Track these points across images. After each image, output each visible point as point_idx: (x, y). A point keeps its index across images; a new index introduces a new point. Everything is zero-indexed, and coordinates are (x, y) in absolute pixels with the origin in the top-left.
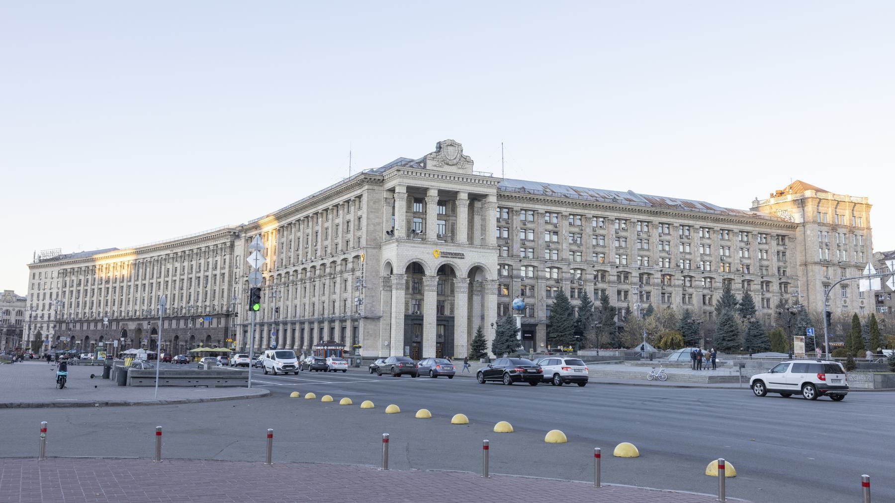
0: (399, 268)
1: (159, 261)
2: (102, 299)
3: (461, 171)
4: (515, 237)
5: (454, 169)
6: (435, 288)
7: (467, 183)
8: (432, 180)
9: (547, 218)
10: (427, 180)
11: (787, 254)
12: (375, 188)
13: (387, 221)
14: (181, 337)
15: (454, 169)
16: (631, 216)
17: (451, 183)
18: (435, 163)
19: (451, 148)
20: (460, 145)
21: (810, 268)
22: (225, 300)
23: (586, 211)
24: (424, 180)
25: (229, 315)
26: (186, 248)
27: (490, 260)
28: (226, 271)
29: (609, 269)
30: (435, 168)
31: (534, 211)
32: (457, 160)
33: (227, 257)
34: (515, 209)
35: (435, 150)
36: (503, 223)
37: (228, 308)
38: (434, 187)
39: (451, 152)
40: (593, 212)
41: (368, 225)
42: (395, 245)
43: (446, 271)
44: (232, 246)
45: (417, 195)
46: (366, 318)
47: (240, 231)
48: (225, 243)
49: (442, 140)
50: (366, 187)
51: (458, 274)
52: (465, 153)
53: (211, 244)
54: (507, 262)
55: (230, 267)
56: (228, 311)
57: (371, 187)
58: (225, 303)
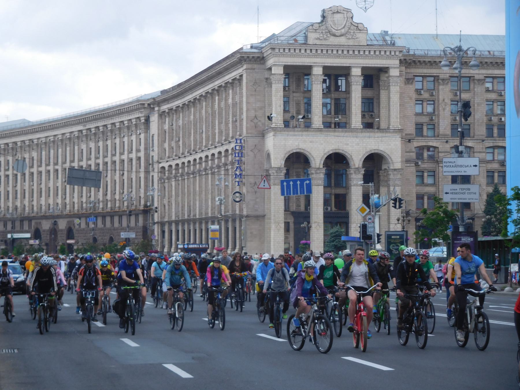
0: (278, 161)
1: (71, 140)
2: (10, 189)
3: (351, 42)
4: (441, 113)
5: (342, 40)
6: (321, 182)
7: (359, 56)
9: (489, 85)
10: (309, 56)
12: (255, 66)
14: (99, 239)
15: (342, 40)
17: (339, 57)
18: (317, 35)
19: (337, 16)
20: (348, 11)
22: (142, 191)
24: (305, 56)
25: (147, 211)
26: (100, 124)
27: (391, 147)
28: (142, 154)
30: (318, 42)
31: (470, 77)
32: (346, 29)
33: (142, 136)
34: (442, 76)
35: (319, 19)
36: (426, 95)
37: (146, 202)
38: (317, 64)
39: (338, 22)
41: (248, 110)
42: (272, 134)
44: (147, 120)
45: (297, 75)
46: (247, 216)
47: (153, 104)
48: (139, 118)
49: (326, 7)
50: (245, 67)
51: (351, 164)
52: (355, 20)
53: (125, 118)
54: (431, 144)
55: (146, 149)
56: (146, 206)
57: (250, 66)
58: (142, 195)
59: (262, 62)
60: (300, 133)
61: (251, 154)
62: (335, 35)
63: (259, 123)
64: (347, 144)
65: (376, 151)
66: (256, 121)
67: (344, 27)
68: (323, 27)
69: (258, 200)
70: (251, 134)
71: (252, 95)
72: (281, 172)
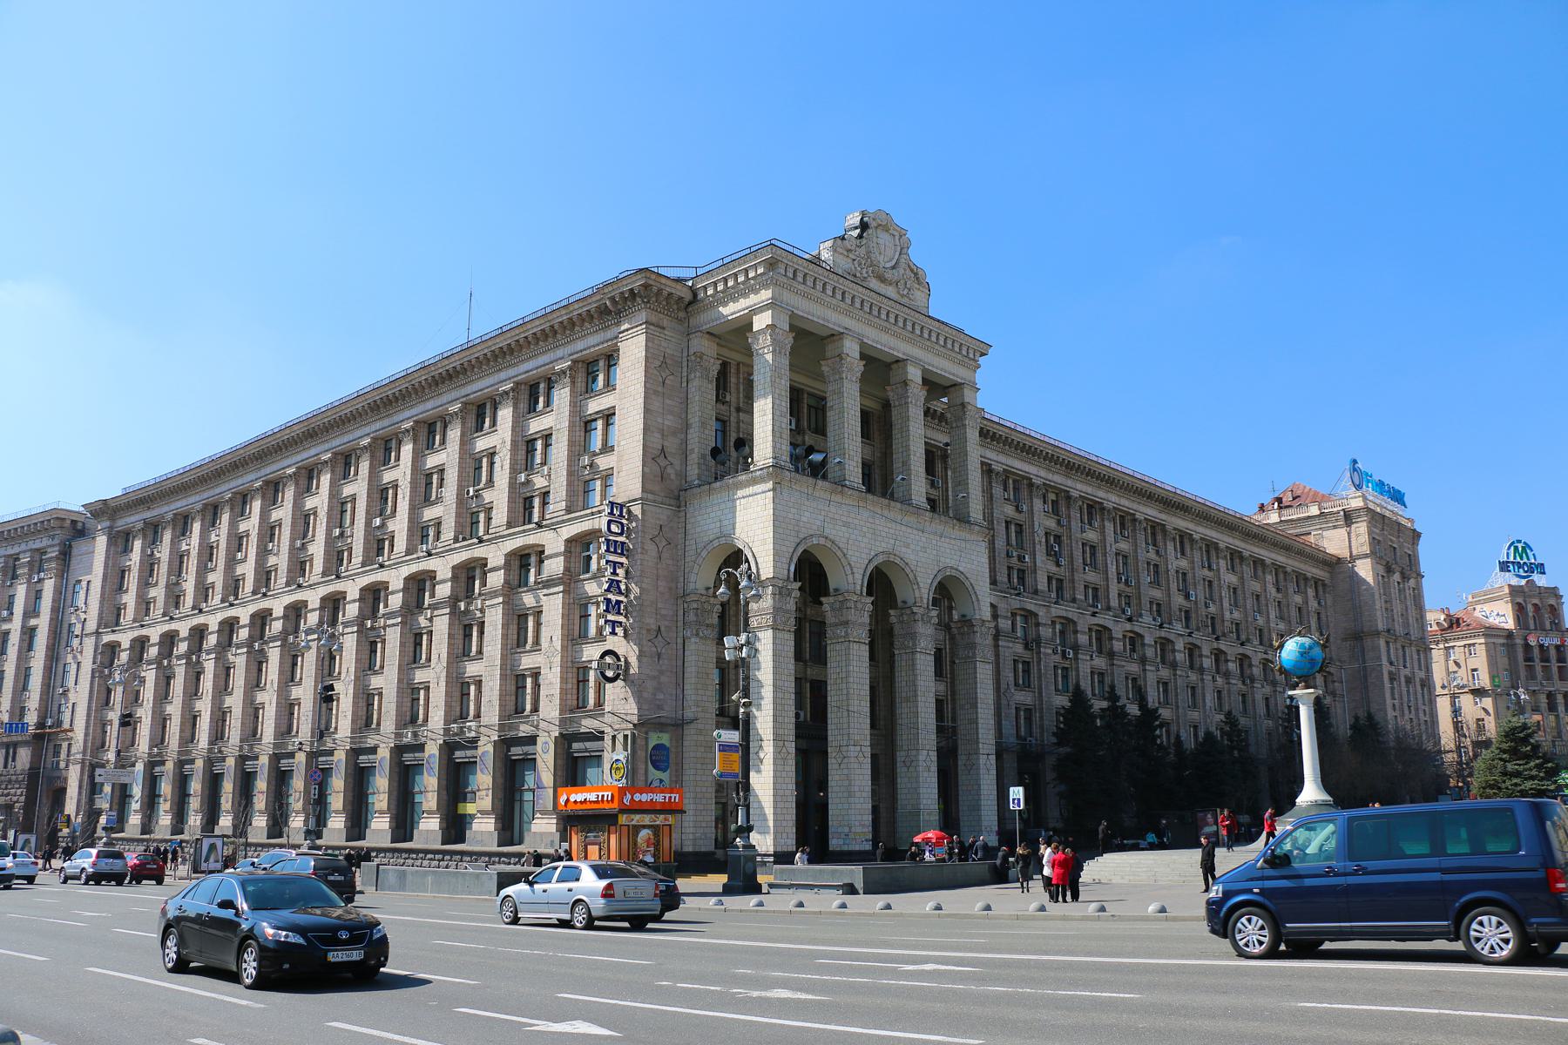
5: (890, 291)
6: (864, 635)
8: (847, 313)
10: (835, 309)
11: (1323, 616)
12: (666, 322)
13: (703, 424)
15: (890, 291)
16: (1135, 506)
17: (886, 330)
19: (884, 238)
21: (1368, 643)
23: (1069, 483)
29: (1110, 625)
40: (1079, 486)
43: (881, 584)
52: (916, 256)
59: (682, 314)
60: (827, 496)
61: (651, 547)
62: (882, 279)
63: (669, 470)
64: (907, 546)
65: (954, 573)
66: (663, 463)
67: (893, 268)
68: (862, 251)
69: (664, 679)
70: (652, 493)
71: (656, 392)
72: (789, 595)
